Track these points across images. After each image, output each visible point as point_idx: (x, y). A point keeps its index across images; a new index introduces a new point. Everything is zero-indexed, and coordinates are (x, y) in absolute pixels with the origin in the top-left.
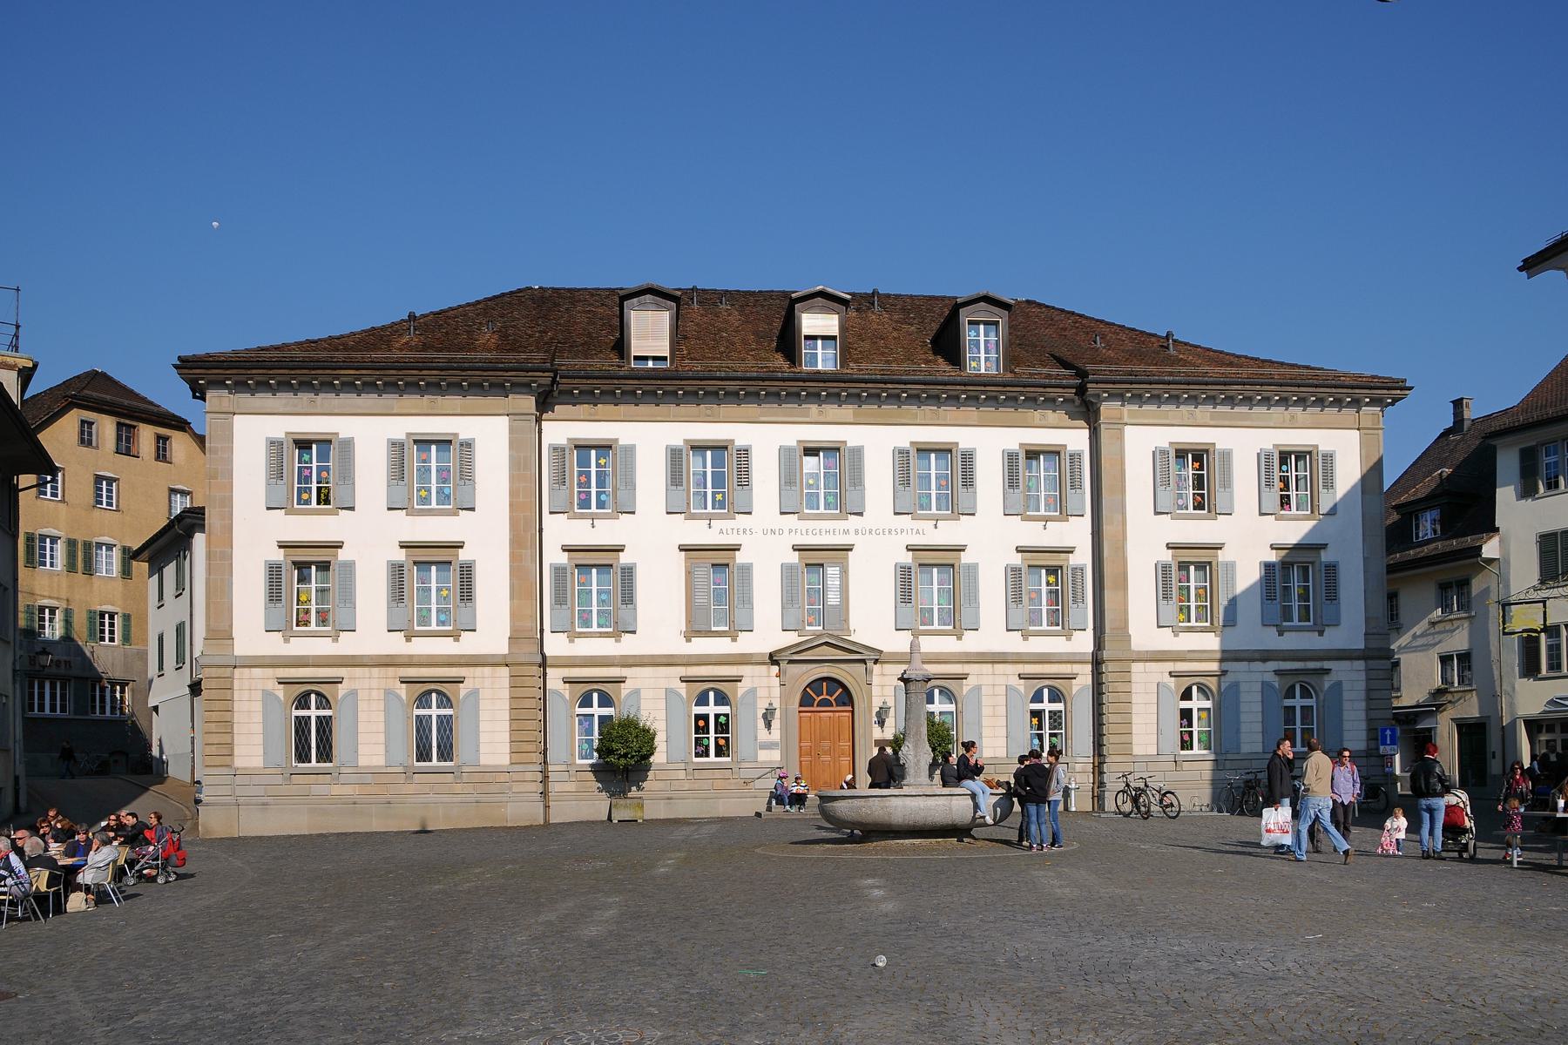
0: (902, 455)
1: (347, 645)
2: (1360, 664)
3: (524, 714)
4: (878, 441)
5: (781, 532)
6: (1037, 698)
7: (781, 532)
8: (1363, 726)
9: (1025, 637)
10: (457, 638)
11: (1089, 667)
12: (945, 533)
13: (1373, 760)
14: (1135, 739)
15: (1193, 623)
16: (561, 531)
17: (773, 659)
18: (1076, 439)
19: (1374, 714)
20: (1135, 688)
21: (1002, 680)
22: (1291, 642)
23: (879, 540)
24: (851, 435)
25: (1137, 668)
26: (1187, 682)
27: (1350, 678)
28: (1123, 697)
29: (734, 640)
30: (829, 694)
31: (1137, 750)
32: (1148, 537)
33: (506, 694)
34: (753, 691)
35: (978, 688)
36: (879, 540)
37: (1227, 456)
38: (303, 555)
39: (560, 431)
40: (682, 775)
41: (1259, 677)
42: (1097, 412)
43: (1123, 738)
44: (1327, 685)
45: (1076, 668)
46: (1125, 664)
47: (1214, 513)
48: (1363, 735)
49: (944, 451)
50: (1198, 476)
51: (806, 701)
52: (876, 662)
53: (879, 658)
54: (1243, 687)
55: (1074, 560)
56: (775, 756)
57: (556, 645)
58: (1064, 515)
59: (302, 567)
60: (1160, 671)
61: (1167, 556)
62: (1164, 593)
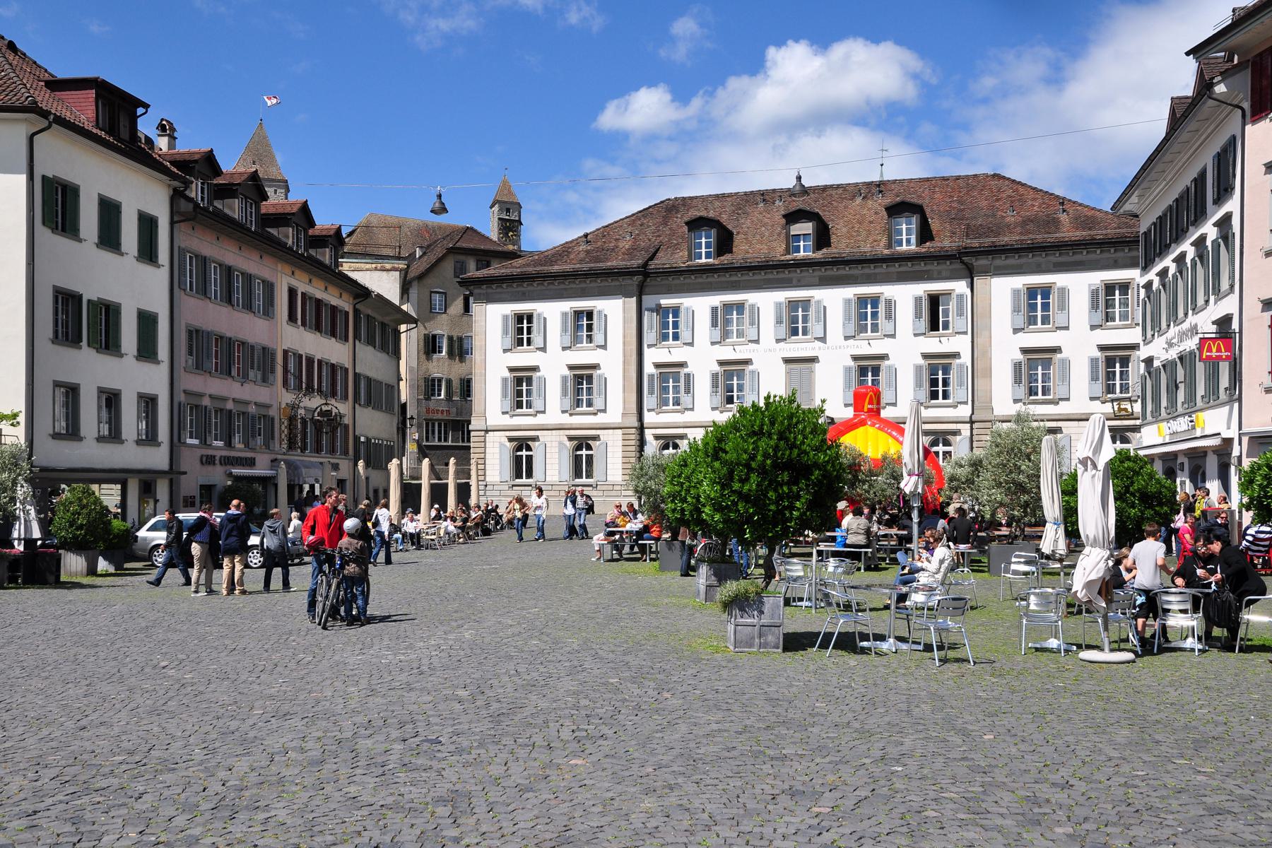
1: (540, 420)
7: (775, 350)
12: (877, 347)
16: (653, 356)
18: (960, 287)
33: (620, 443)
39: (648, 300)
61: (1020, 357)
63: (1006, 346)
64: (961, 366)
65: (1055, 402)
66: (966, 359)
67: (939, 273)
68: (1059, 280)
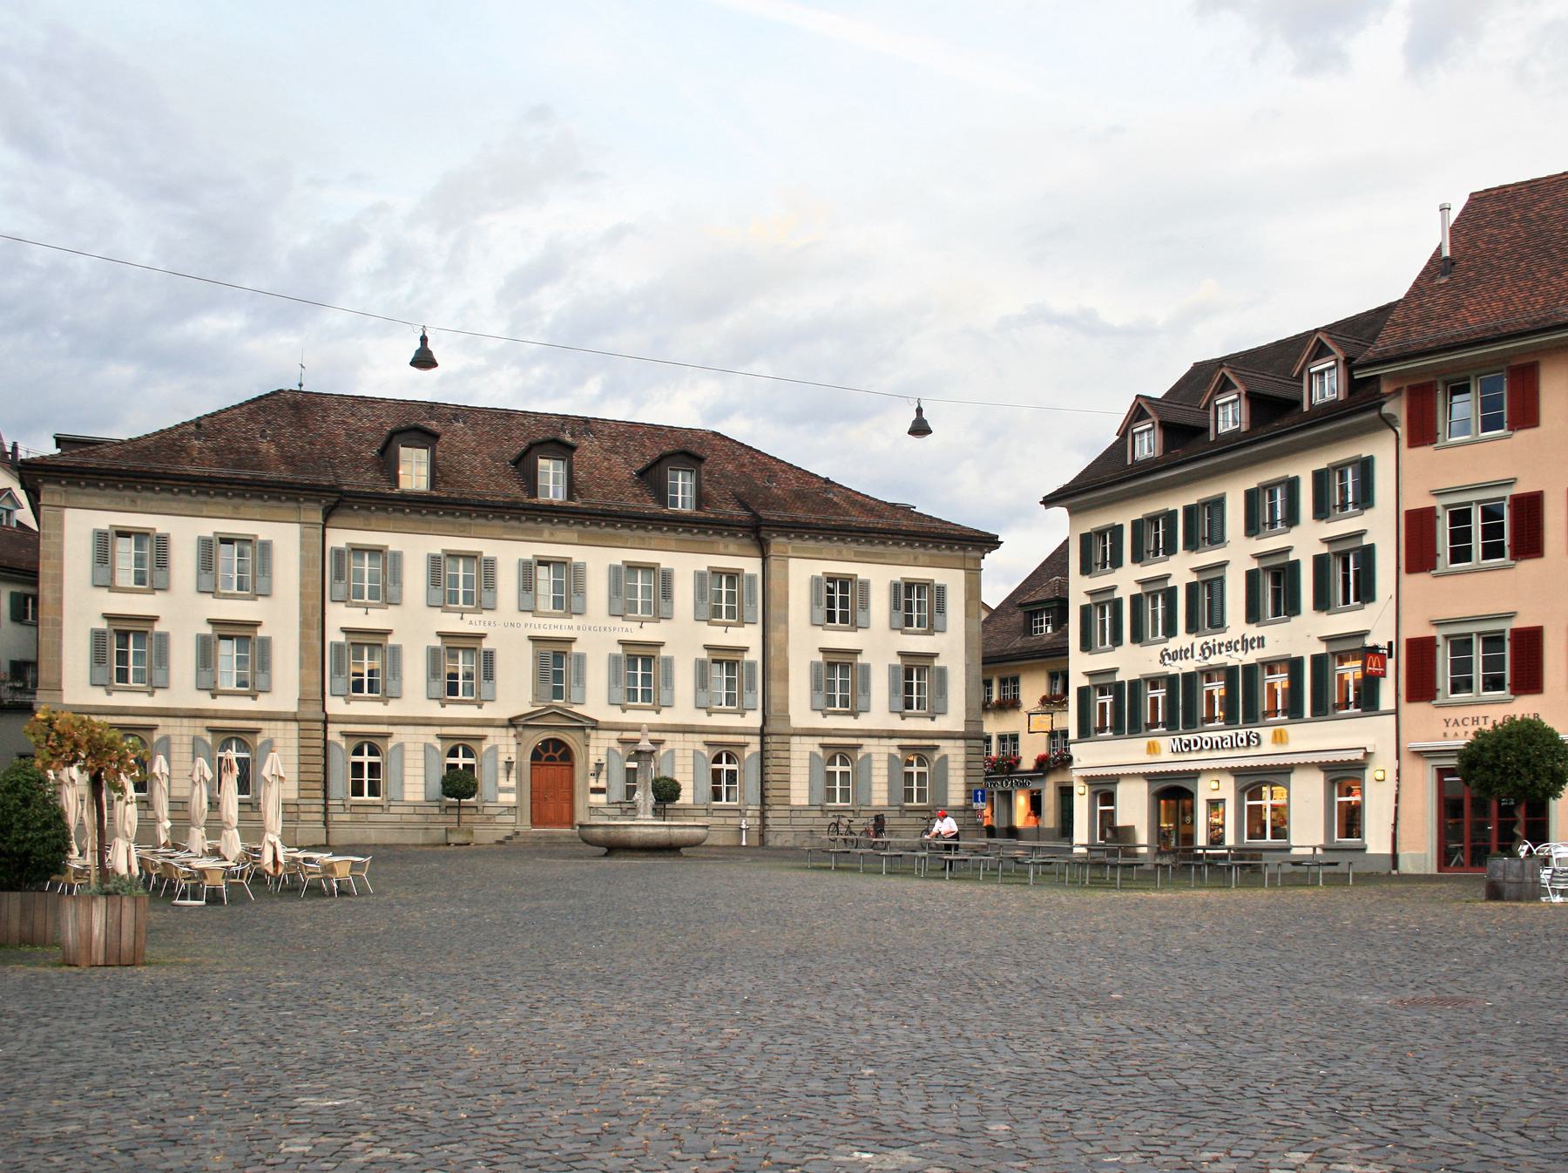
0: (615, 571)
2: (961, 743)
3: (310, 760)
4: (598, 561)
5: (519, 625)
6: (718, 760)
7: (519, 625)
8: (962, 787)
9: (709, 714)
10: (254, 698)
11: (757, 739)
12: (649, 632)
13: (968, 813)
14: (793, 794)
15: (838, 708)
17: (512, 723)
18: (750, 566)
19: (972, 780)
20: (793, 755)
21: (690, 746)
22: (912, 725)
23: (597, 636)
24: (576, 553)
25: (795, 740)
26: (831, 752)
27: (954, 753)
28: (784, 762)
29: (480, 707)
30: (553, 756)
31: (794, 801)
32: (806, 641)
33: (295, 743)
34: (495, 748)
35: (672, 751)
36: (597, 636)
37: (865, 585)
38: (124, 626)
40: (436, 811)
41: (885, 750)
42: (768, 545)
43: (783, 793)
44: (936, 757)
45: (748, 739)
46: (785, 739)
47: (855, 627)
48: (962, 795)
49: (649, 568)
50: (840, 602)
51: (536, 755)
52: (593, 728)
53: (596, 726)
54: (874, 757)
55: (747, 657)
56: (511, 798)
57: (335, 706)
58: (741, 624)
59: (123, 635)
60: (812, 744)
62: (816, 687)
63: (806, 641)
64: (752, 665)
65: (855, 714)
66: (754, 655)
67: (726, 546)
68: (861, 571)
